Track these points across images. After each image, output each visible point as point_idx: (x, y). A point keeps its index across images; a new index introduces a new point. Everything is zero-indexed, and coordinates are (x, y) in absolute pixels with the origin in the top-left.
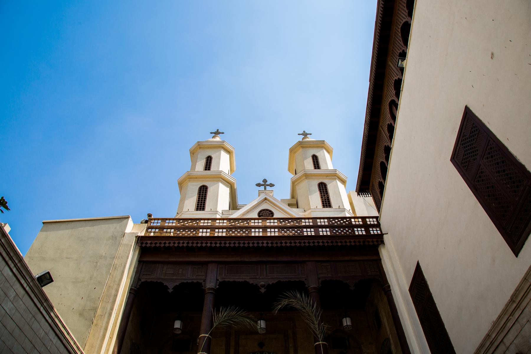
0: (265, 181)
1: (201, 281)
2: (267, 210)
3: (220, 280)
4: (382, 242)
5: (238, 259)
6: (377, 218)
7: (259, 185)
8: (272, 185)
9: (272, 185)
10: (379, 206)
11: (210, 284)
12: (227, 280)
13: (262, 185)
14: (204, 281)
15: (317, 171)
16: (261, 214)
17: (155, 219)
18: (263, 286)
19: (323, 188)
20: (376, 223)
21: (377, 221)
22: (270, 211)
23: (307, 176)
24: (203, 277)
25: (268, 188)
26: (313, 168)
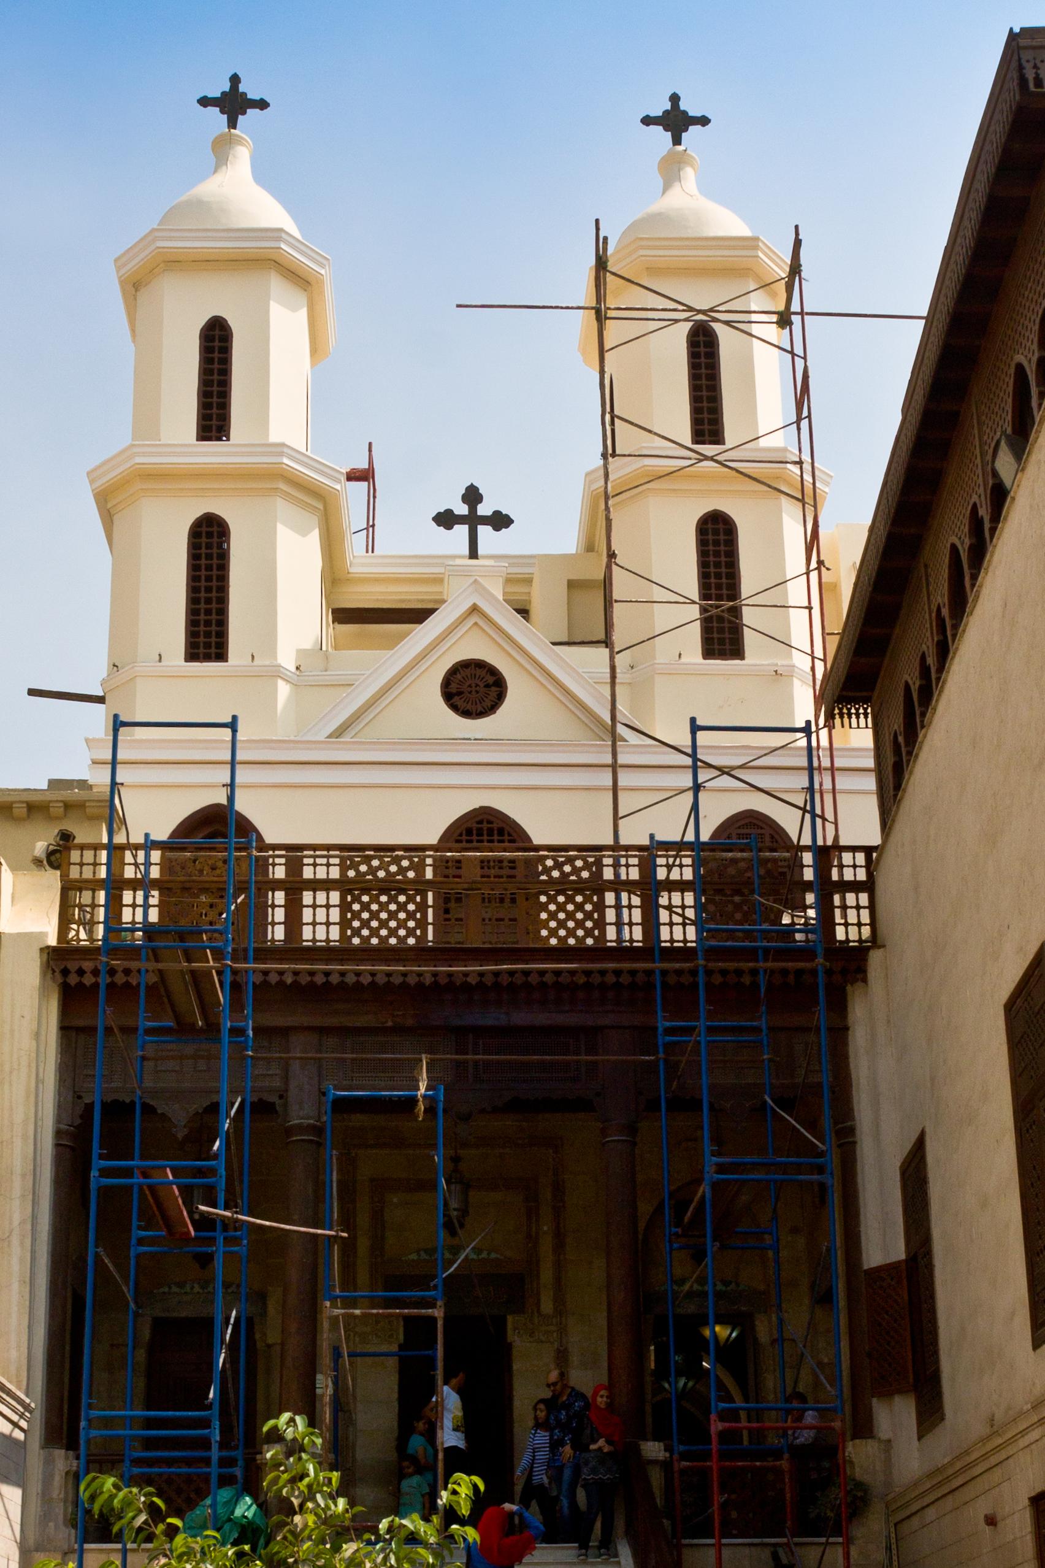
0: (472, 496)
1: (274, 1098)
6: (868, 850)
7: (445, 519)
8: (500, 521)
9: (500, 521)
14: (281, 1097)
16: (453, 688)
17: (82, 847)
20: (862, 875)
21: (869, 865)
24: (277, 1083)
25: (484, 531)
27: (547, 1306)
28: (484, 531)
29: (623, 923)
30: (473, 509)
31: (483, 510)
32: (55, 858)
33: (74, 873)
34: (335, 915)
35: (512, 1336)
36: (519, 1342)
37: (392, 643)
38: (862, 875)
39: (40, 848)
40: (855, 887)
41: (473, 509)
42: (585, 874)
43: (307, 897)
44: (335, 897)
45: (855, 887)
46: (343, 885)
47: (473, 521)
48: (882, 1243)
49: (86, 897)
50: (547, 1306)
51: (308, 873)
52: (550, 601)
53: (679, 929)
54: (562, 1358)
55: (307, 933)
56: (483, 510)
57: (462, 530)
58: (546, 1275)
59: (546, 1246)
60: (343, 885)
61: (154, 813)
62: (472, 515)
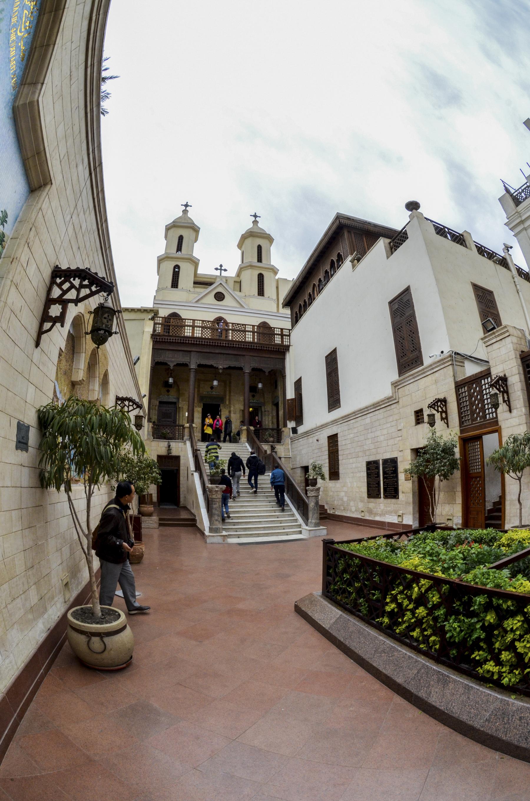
0: (221, 266)
1: (188, 363)
2: (221, 293)
3: (198, 363)
4: (288, 350)
5: (208, 351)
6: (289, 330)
7: (217, 269)
8: (225, 270)
9: (225, 270)
10: (293, 326)
11: (193, 366)
12: (202, 363)
15: (259, 264)
18: (221, 369)
19: (261, 277)
22: (223, 294)
23: (251, 266)
24: (189, 360)
26: (256, 260)
27: (227, 403)
29: (249, 338)
32: (153, 319)
33: (156, 321)
34: (200, 332)
35: (221, 408)
36: (222, 407)
37: (207, 288)
38: (288, 334)
39: (150, 317)
40: (287, 335)
42: (241, 329)
43: (196, 328)
44: (200, 329)
45: (287, 335)
46: (202, 327)
47: (221, 270)
48: (290, 394)
49: (158, 326)
50: (227, 403)
51: (196, 324)
52: (231, 283)
54: (230, 412)
55: (195, 335)
56: (223, 268)
58: (227, 397)
59: (228, 392)
60: (202, 327)
61: (164, 313)
62: (221, 268)
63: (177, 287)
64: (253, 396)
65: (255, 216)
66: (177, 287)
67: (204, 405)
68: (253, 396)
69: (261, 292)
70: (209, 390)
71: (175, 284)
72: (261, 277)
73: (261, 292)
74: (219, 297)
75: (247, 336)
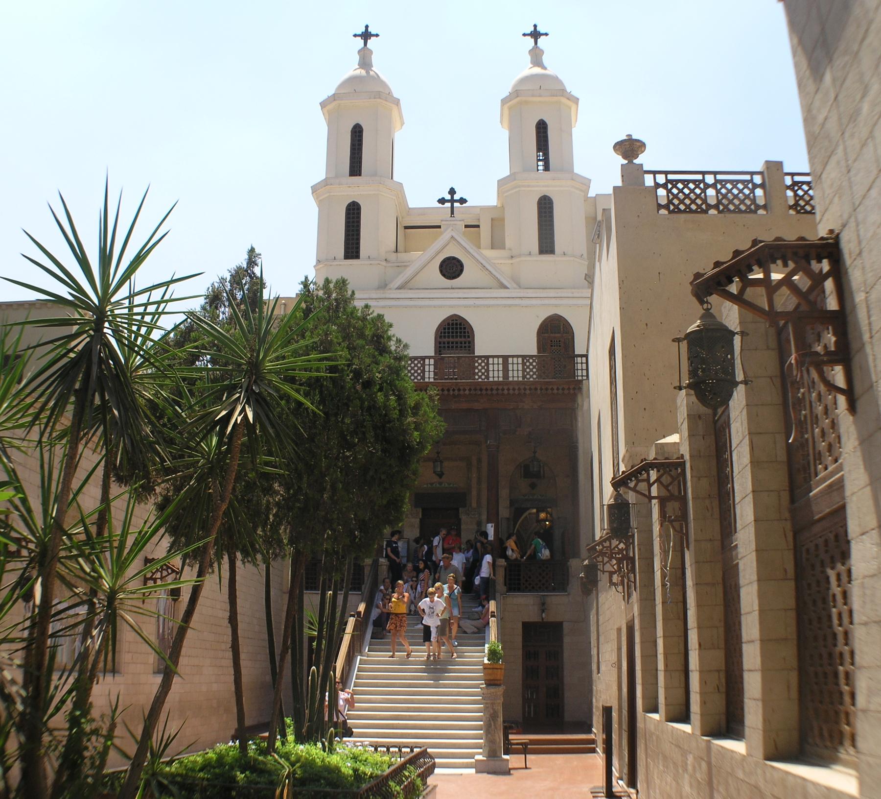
0: (452, 192)
2: (454, 258)
8: (462, 201)
13: (448, 201)
19: (545, 206)
22: (459, 261)
25: (456, 205)
27: (474, 505)
28: (456, 205)
30: (452, 197)
31: (456, 197)
36: (463, 517)
40: (582, 356)
41: (452, 197)
47: (452, 201)
50: (474, 505)
53: (516, 374)
56: (456, 197)
57: (448, 205)
58: (474, 493)
63: (357, 257)
64: (533, 486)
65: (535, 34)
66: (357, 257)
67: (423, 510)
68: (533, 486)
69: (547, 245)
70: (436, 479)
71: (352, 250)
72: (545, 206)
73: (547, 245)
74: (451, 268)
75: (491, 367)
